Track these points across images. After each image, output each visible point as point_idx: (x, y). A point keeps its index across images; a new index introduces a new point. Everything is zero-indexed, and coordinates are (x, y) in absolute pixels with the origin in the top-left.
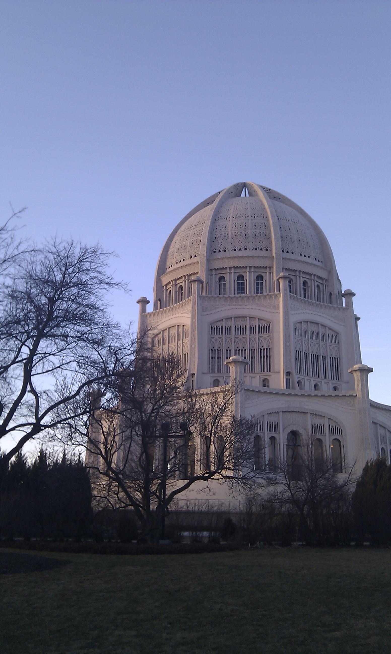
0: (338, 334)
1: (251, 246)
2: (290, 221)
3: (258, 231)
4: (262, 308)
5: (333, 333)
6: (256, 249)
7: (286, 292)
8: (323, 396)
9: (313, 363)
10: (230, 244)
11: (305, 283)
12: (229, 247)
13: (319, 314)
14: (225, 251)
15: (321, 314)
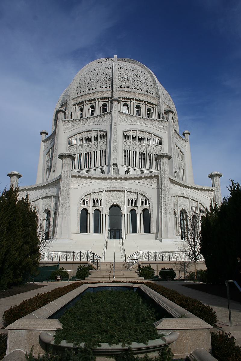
0: (161, 139)
1: (99, 86)
2: (129, 70)
3: (105, 77)
4: (101, 123)
5: (158, 138)
6: (102, 88)
7: (115, 110)
8: (136, 178)
9: (140, 159)
10: (86, 87)
11: (138, 107)
12: (87, 88)
13: (146, 125)
14: (83, 92)
15: (148, 126)
